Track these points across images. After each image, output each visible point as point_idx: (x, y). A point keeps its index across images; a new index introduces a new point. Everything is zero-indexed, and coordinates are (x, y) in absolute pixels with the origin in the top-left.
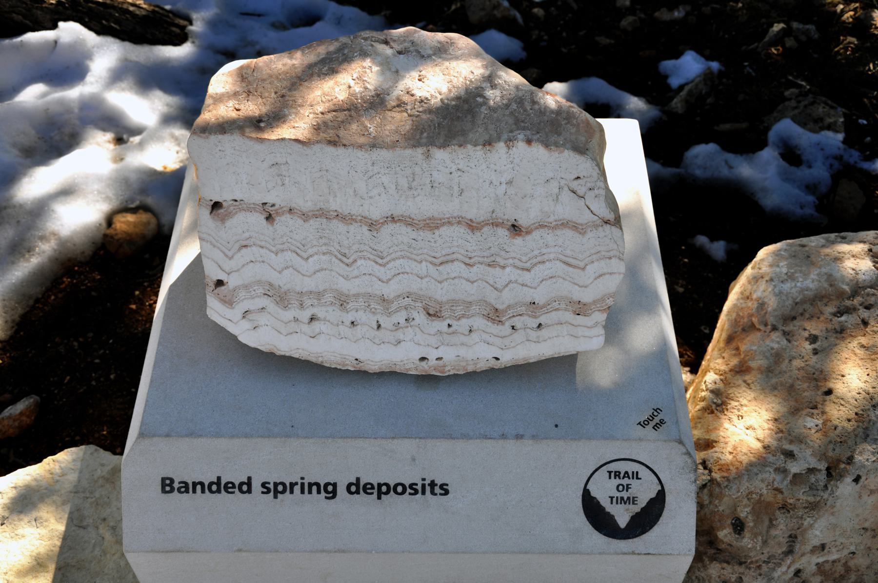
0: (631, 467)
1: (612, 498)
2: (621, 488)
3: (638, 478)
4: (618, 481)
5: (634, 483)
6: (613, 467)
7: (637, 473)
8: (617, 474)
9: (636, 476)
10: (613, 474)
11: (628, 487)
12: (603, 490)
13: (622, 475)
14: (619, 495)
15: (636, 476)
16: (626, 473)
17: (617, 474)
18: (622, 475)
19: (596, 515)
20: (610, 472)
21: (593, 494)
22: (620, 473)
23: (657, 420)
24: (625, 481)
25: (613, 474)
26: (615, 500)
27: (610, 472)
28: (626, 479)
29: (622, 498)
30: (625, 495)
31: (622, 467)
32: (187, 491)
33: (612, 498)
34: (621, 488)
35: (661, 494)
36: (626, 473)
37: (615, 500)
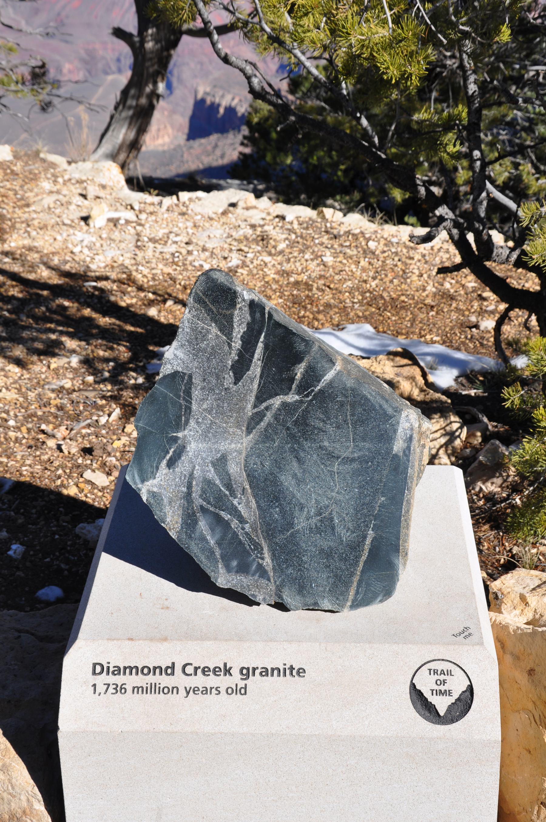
1: (432, 691)
2: (439, 682)
3: (451, 675)
4: (436, 677)
6: (432, 666)
8: (435, 672)
9: (449, 673)
10: (432, 672)
11: (444, 682)
12: (426, 684)
13: (439, 673)
14: (438, 688)
15: (449, 673)
17: (435, 672)
18: (439, 673)
20: (430, 670)
24: (442, 677)
25: (432, 672)
26: (434, 692)
27: (430, 670)
29: (440, 691)
30: (442, 688)
31: (439, 666)
33: (432, 691)
34: (439, 682)
35: (471, 689)
36: (443, 670)
37: (434, 692)
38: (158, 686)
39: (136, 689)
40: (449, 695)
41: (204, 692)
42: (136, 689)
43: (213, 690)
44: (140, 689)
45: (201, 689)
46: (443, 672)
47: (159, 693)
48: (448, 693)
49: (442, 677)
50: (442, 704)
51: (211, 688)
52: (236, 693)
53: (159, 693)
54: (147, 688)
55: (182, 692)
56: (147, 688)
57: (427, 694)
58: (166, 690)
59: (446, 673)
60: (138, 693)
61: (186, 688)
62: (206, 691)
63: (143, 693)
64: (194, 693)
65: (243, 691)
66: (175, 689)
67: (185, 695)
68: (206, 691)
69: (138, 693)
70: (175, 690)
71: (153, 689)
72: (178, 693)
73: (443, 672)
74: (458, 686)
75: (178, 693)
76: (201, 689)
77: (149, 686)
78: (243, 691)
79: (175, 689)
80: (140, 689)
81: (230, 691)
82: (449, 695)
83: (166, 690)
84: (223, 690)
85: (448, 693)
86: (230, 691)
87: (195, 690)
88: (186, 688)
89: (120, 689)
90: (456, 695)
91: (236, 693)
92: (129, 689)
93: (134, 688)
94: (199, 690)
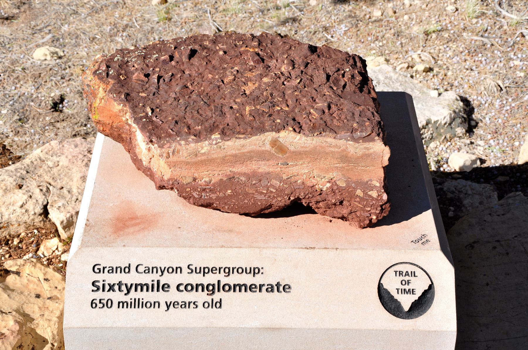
0: (410, 268)
1: (398, 289)
4: (402, 278)
5: (412, 279)
7: (414, 272)
8: (401, 273)
10: (398, 273)
11: (408, 282)
12: (392, 284)
13: (404, 274)
14: (403, 287)
15: (414, 274)
16: (407, 272)
18: (404, 274)
19: (386, 299)
20: (396, 272)
21: (385, 287)
22: (403, 273)
23: (424, 240)
24: (407, 278)
25: (398, 273)
26: (400, 291)
27: (396, 272)
28: (407, 276)
30: (407, 287)
31: (404, 268)
32: (272, 291)
33: (398, 289)
35: (431, 287)
36: (407, 272)
37: (400, 291)
38: (141, 301)
39: (121, 304)
40: (413, 294)
41: (183, 306)
42: (121, 304)
43: (192, 305)
44: (125, 304)
45: (180, 304)
46: (407, 274)
47: (142, 307)
48: (412, 292)
49: (407, 278)
50: (406, 302)
51: (189, 303)
52: (212, 307)
53: (142, 307)
54: (131, 302)
55: (163, 307)
56: (131, 302)
57: (394, 293)
58: (148, 305)
59: (410, 275)
60: (123, 307)
61: (166, 302)
62: (185, 305)
63: (127, 307)
64: (174, 307)
65: (218, 305)
66: (156, 304)
67: (166, 309)
68: (185, 305)
69: (123, 307)
70: (157, 304)
71: (138, 304)
72: (159, 307)
73: (407, 274)
74: (420, 286)
75: (159, 307)
76: (180, 304)
77: (133, 301)
78: (218, 305)
79: (156, 304)
80: (125, 304)
81: (206, 305)
82: (413, 294)
83: (148, 305)
84: (200, 305)
85: (412, 292)
86: (206, 305)
87: (175, 304)
88: (166, 302)
89: (108, 304)
90: (419, 293)
91: (212, 307)
92: (115, 304)
93: (119, 303)
94: (178, 304)
